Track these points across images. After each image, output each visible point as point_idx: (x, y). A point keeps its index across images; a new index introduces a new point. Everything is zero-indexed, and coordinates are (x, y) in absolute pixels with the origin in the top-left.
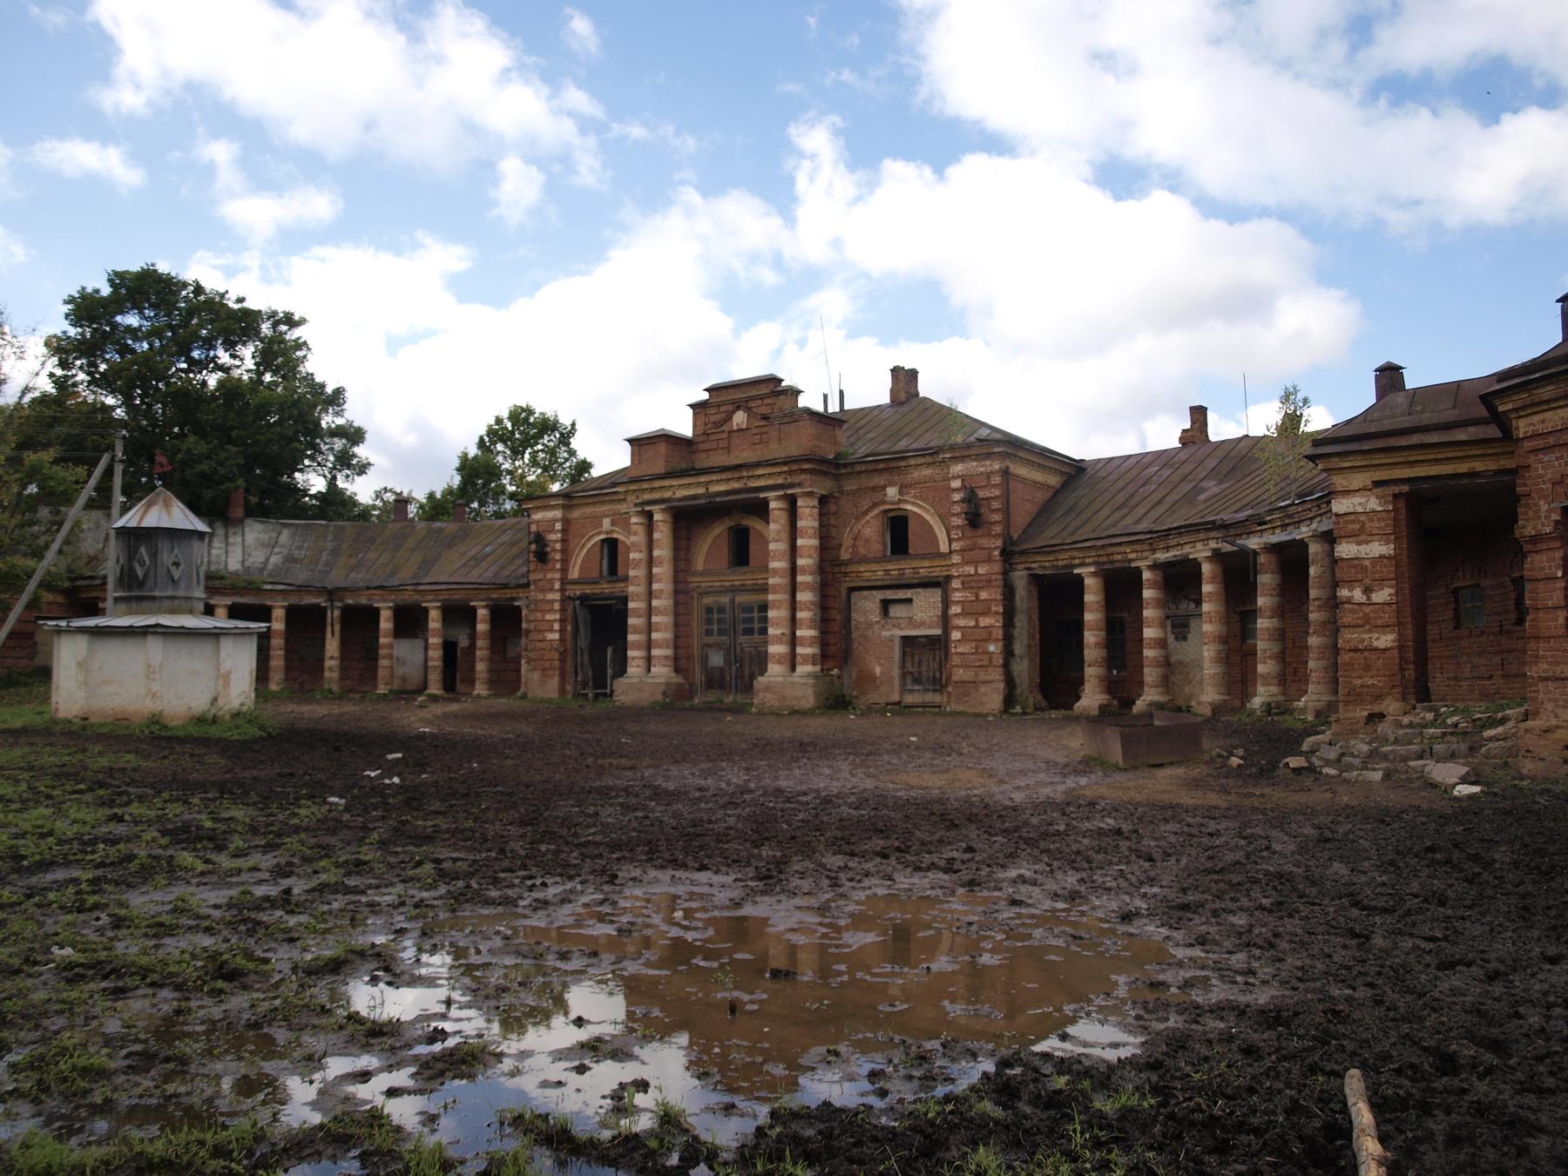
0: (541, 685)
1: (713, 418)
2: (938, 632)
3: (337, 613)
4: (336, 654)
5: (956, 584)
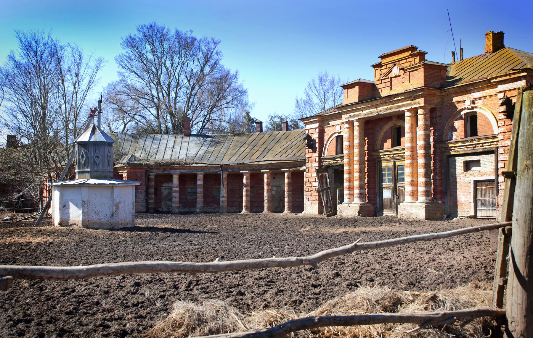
0: (311, 208)
1: (384, 71)
2: (493, 177)
3: (225, 176)
4: (225, 195)
5: (501, 151)
